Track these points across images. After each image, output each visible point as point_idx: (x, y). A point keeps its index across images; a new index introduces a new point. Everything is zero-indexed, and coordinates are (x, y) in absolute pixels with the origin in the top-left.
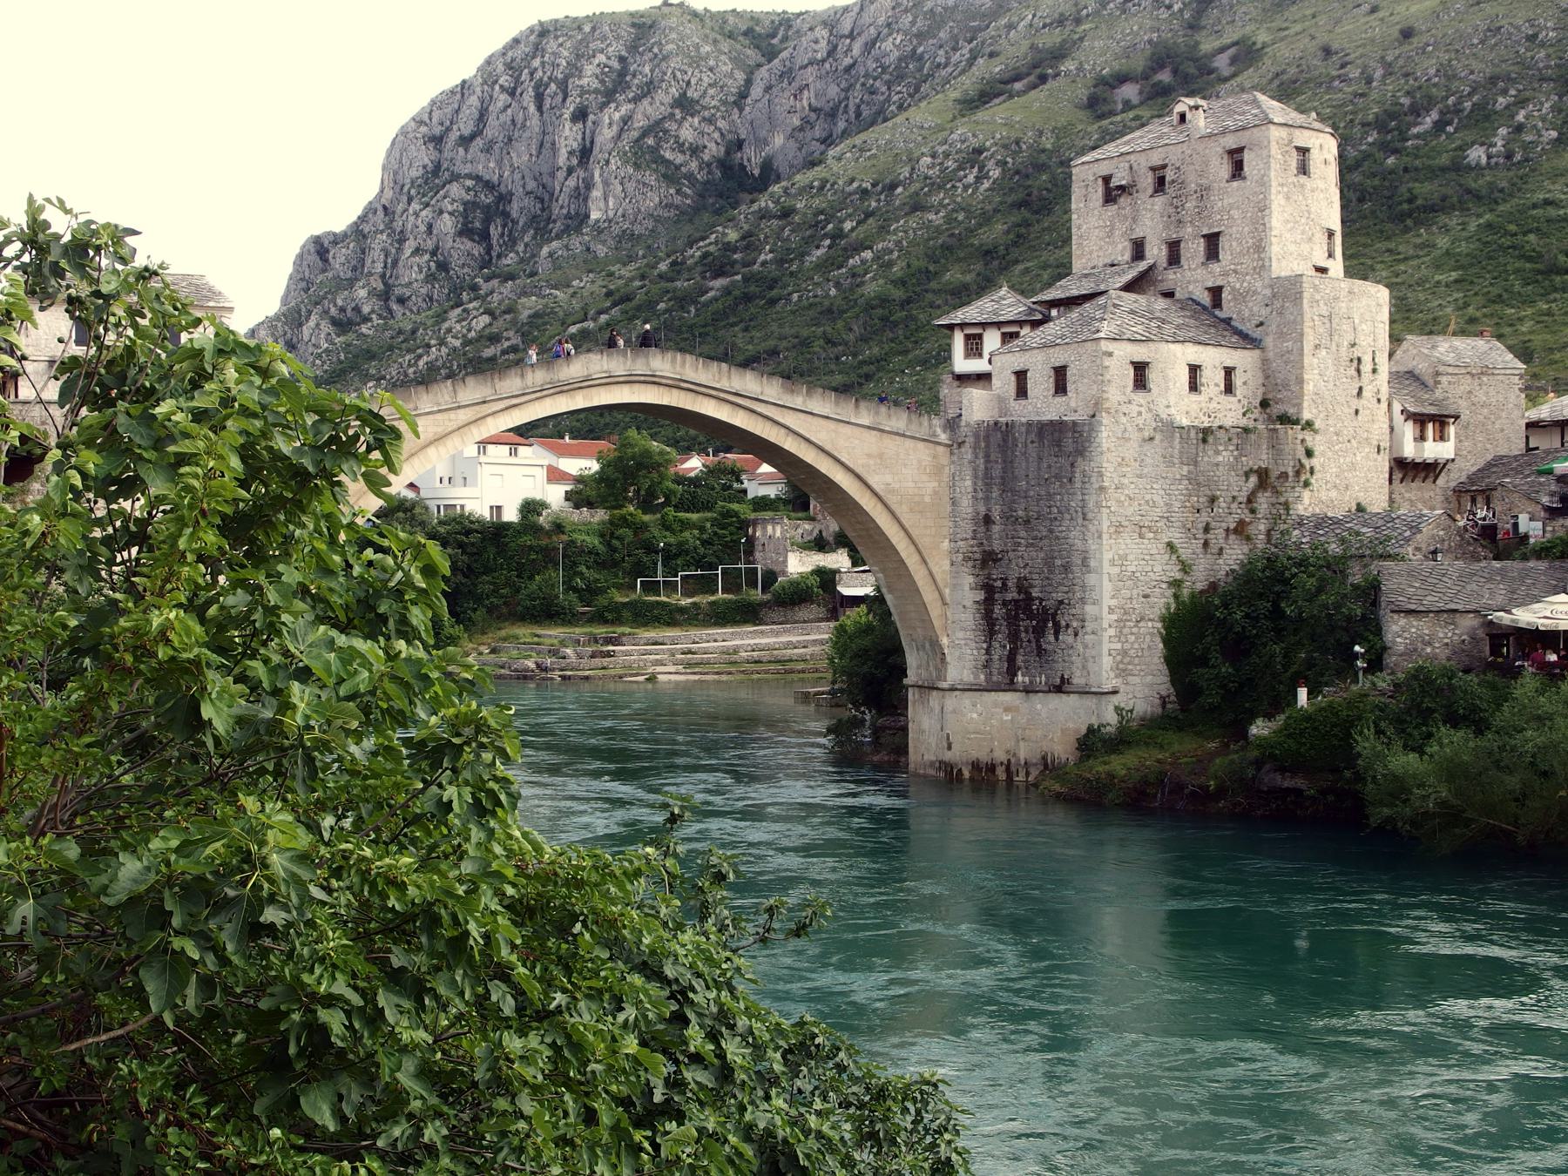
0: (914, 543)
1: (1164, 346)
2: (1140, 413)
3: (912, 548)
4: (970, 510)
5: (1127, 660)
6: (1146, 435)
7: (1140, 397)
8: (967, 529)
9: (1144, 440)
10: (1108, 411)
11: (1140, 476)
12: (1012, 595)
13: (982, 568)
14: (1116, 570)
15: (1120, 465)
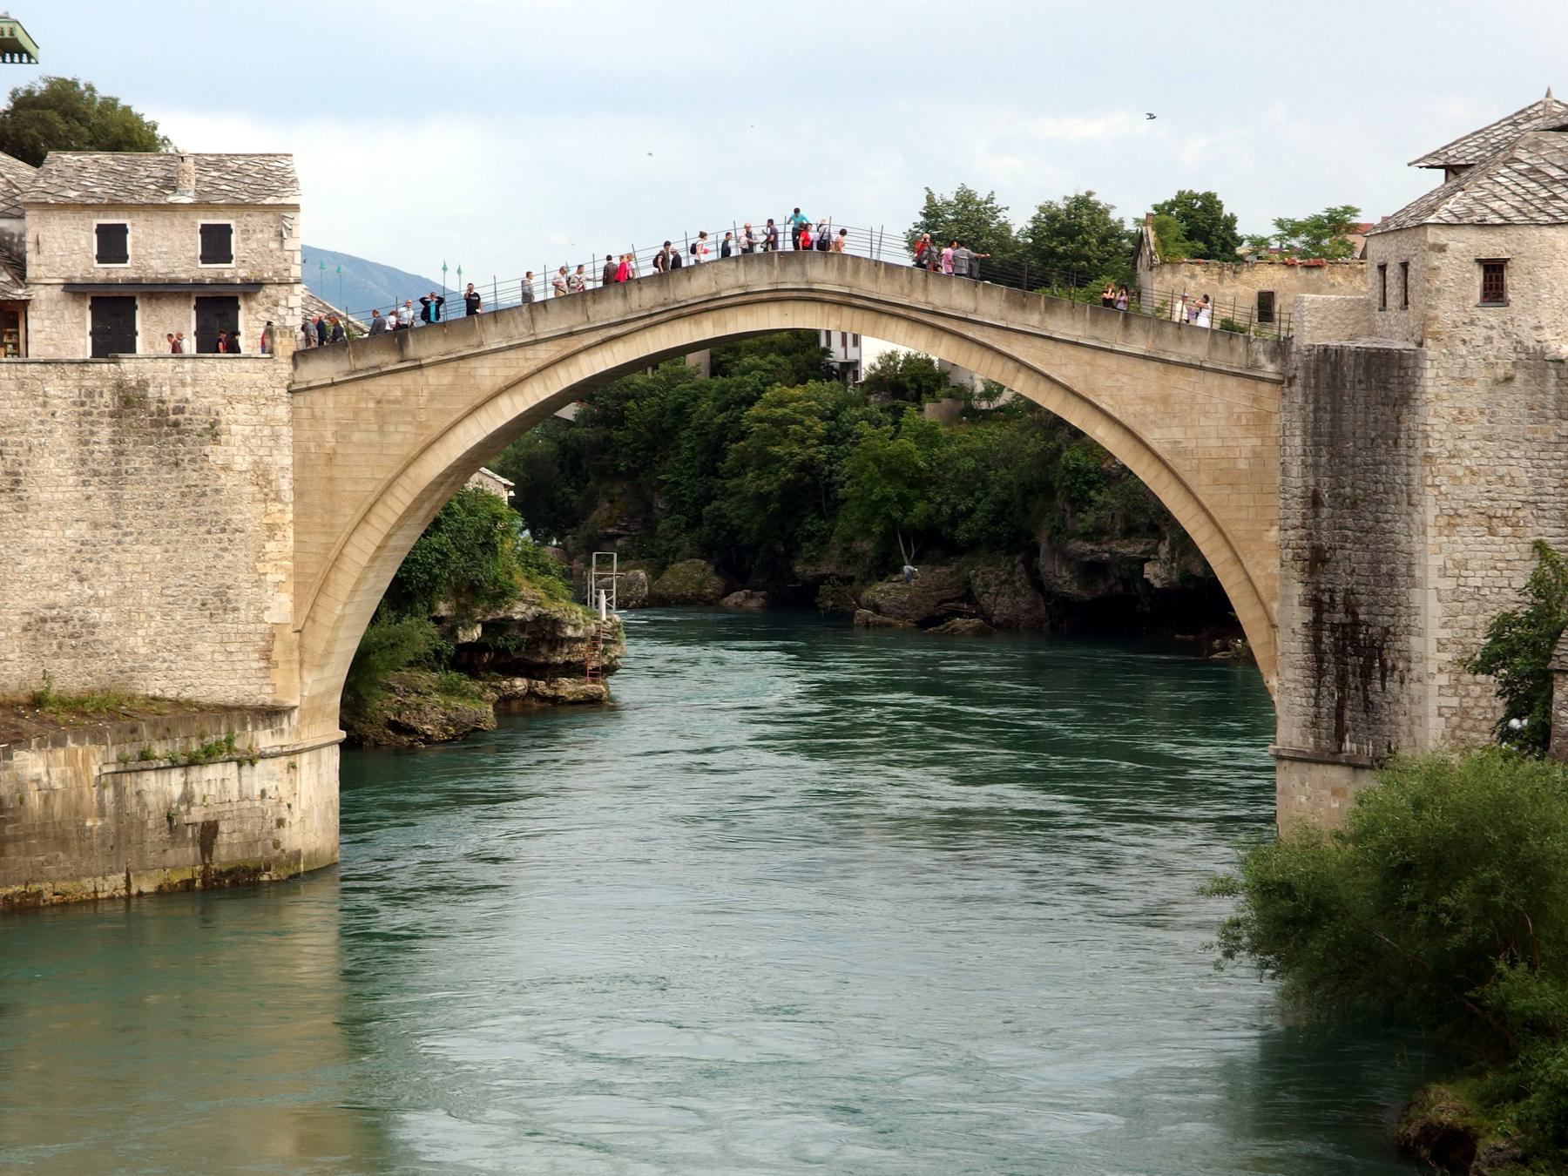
0: (1221, 531)
1: (1535, 232)
2: (1489, 340)
3: (1219, 540)
4: (1299, 483)
5: (1468, 724)
6: (1500, 373)
7: (1492, 315)
8: (1297, 510)
9: (1497, 382)
10: (1436, 337)
11: (1490, 438)
12: (1339, 617)
13: (1312, 573)
14: (1450, 584)
15: (1456, 420)
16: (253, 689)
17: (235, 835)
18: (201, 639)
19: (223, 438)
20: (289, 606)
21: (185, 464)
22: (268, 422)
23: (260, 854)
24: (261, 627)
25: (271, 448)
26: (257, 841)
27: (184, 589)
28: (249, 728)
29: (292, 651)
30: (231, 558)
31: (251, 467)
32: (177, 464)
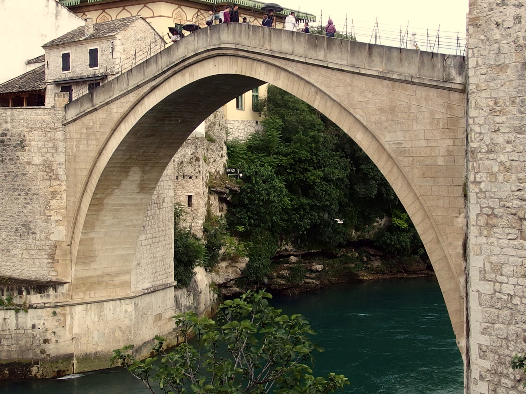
16: (45, 273)
17: (13, 347)
18: (15, 247)
19: (27, 148)
20: (64, 232)
21: (7, 161)
22: (51, 140)
23: (31, 356)
24: (48, 242)
25: (53, 153)
26: (29, 350)
27: (6, 222)
28: (24, 293)
29: (66, 255)
30: (31, 208)
31: (42, 163)
32: (2, 161)
